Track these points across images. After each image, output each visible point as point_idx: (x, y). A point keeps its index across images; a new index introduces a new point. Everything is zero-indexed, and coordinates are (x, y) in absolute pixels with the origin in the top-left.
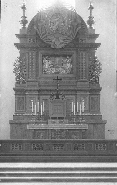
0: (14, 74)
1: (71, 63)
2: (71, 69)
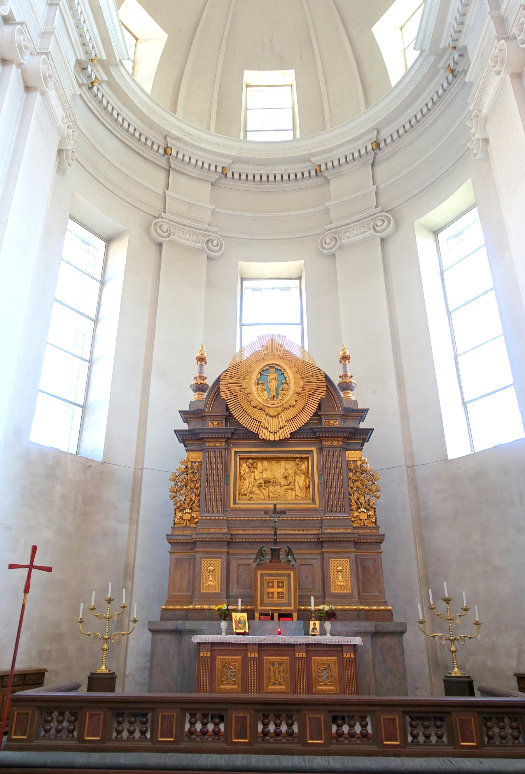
0: (172, 502)
1: (306, 474)
2: (306, 488)
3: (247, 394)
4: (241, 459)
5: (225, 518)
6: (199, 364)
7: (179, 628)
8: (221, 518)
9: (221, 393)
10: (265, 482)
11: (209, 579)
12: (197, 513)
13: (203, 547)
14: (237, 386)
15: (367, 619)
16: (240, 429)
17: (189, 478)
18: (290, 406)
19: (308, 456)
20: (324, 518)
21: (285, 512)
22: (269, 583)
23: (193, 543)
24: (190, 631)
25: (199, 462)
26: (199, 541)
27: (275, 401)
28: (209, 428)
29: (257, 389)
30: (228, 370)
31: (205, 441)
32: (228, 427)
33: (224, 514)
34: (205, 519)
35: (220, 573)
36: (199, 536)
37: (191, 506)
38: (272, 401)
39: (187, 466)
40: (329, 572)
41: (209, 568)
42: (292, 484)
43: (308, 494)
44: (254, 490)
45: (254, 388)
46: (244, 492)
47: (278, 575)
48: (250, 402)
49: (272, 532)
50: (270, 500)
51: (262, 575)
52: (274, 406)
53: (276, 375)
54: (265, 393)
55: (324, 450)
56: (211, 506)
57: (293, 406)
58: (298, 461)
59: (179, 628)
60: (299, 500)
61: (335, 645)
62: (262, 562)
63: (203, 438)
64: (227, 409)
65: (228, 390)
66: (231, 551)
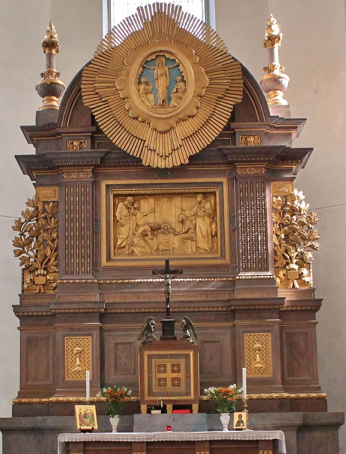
0: (18, 261)
1: (213, 217)
3: (124, 99)
4: (115, 196)
5: (96, 281)
6: (47, 52)
7: (38, 426)
8: (90, 281)
9: (84, 98)
10: (152, 229)
11: (75, 363)
12: (55, 274)
13: (66, 321)
14: (108, 87)
15: (292, 409)
16: (113, 151)
17: (40, 226)
18: (189, 117)
19: (216, 190)
20: (238, 277)
21: (182, 271)
22: (159, 366)
23: (50, 316)
24: (54, 430)
25: (54, 202)
26: (59, 313)
27: (166, 108)
28: (68, 151)
29: (139, 90)
30: (92, 62)
31: (61, 170)
32: (96, 150)
33: (93, 275)
34: (66, 283)
35: (90, 355)
36: (59, 307)
37: (45, 265)
38: (161, 108)
39: (37, 209)
40: (244, 350)
41: (75, 349)
42: (192, 230)
43: (215, 245)
44: (135, 240)
45: (133, 88)
46: (121, 244)
47: (172, 356)
48: (128, 111)
49: (164, 299)
50: (160, 255)
51: (150, 357)
52: (164, 116)
53: (166, 68)
54: (151, 97)
55: (238, 181)
56: (75, 265)
57: (192, 117)
58: (199, 198)
59: (39, 425)
60: (201, 253)
61: (249, 441)
62: (150, 339)
63: (58, 167)
64: (94, 122)
65: (93, 93)
66: (107, 326)
